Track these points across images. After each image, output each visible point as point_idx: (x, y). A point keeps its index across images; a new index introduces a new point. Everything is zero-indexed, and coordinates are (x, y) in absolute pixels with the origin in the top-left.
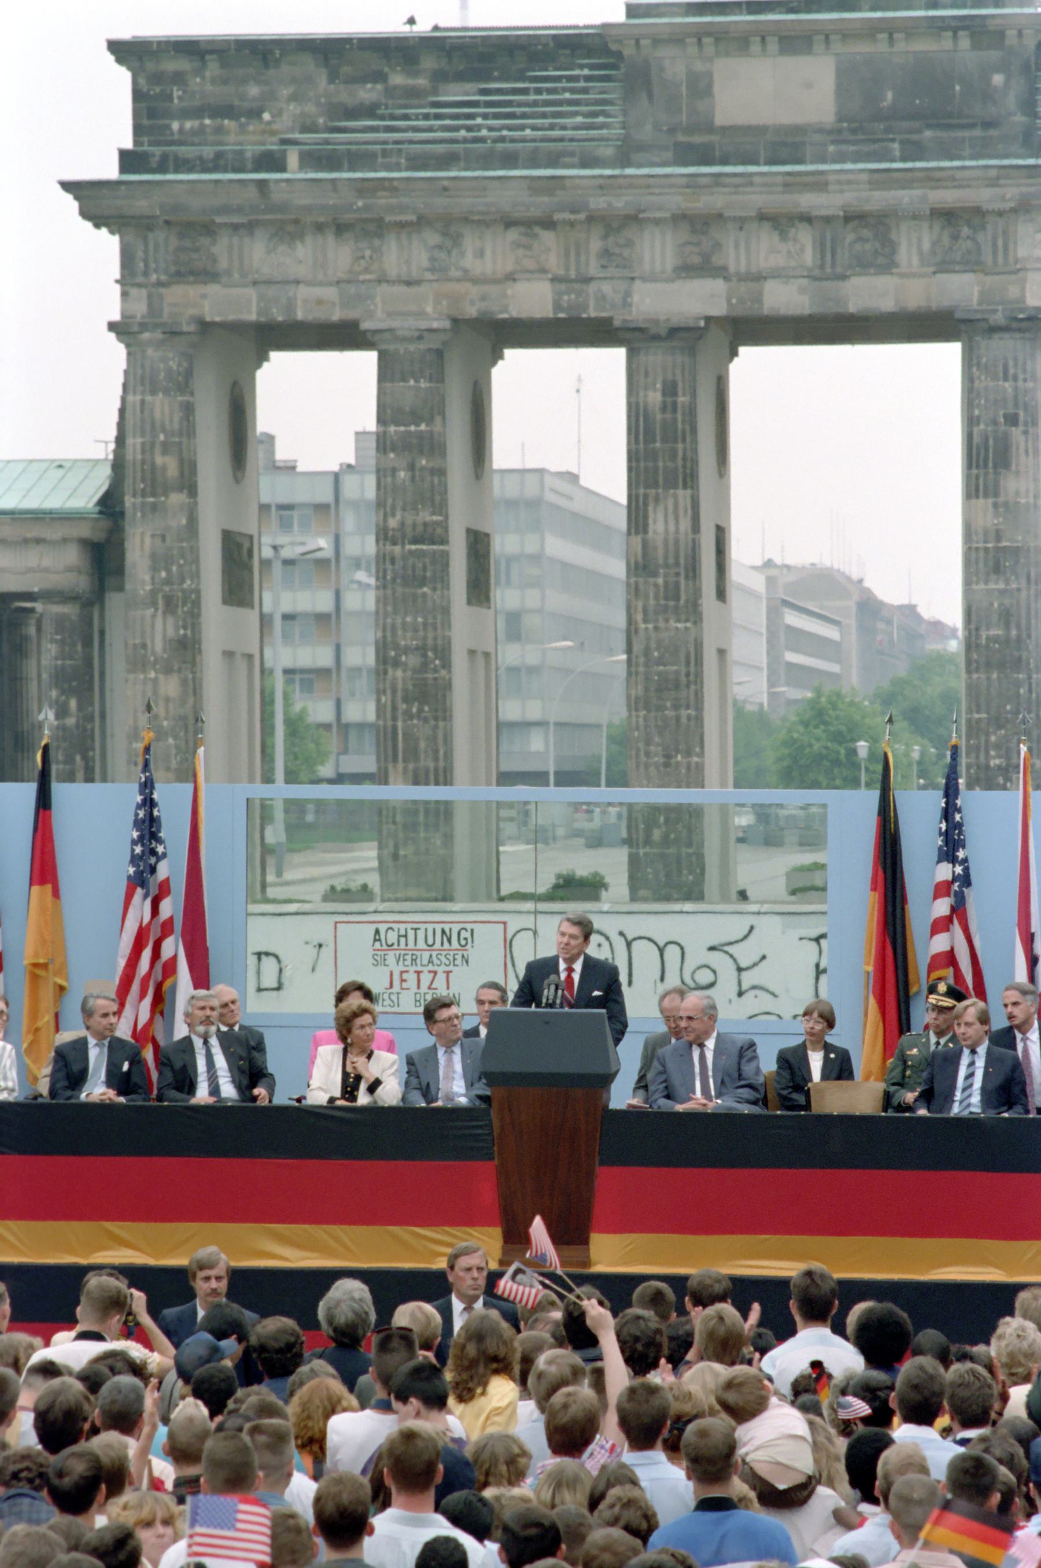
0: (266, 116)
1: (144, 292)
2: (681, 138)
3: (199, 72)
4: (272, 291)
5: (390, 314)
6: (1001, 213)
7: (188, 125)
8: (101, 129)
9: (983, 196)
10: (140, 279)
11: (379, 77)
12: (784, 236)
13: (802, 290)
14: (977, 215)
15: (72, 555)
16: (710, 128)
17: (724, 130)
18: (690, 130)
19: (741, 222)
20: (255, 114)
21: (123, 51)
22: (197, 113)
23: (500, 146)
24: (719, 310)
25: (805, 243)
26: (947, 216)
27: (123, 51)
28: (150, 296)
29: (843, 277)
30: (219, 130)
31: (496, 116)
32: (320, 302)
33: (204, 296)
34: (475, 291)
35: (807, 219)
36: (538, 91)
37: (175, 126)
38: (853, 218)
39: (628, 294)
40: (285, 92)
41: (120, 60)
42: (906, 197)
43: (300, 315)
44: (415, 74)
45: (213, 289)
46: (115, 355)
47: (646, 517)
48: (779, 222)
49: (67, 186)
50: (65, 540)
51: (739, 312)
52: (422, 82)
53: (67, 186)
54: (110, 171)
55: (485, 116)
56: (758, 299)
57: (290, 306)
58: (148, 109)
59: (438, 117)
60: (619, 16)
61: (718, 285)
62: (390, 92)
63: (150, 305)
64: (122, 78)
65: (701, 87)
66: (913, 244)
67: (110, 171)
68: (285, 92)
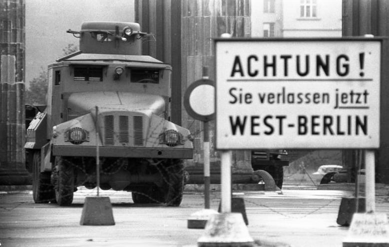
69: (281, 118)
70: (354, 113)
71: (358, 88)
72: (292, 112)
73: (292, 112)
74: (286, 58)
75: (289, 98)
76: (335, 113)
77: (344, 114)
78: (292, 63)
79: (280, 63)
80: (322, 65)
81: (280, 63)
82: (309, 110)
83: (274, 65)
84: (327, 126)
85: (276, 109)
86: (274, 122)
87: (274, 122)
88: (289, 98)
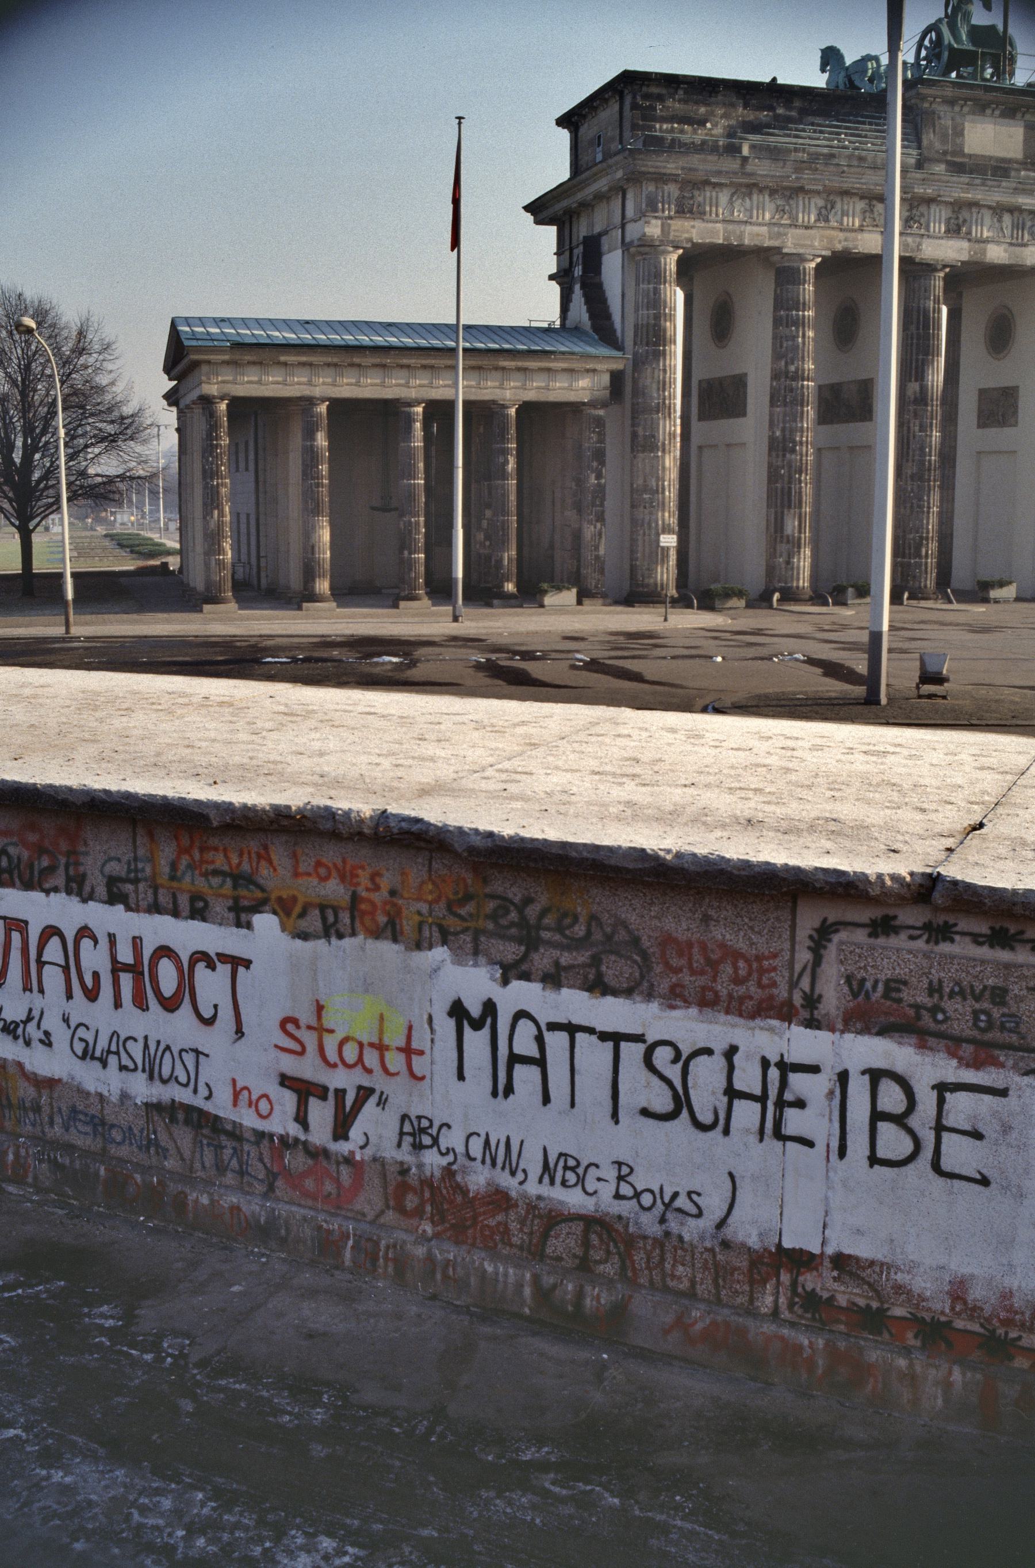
0: (708, 125)
1: (659, 222)
2: (949, 158)
3: (672, 96)
4: (730, 227)
5: (795, 245)
7: (665, 126)
10: (660, 214)
11: (771, 108)
13: (1006, 251)
16: (964, 155)
17: (970, 156)
18: (954, 153)
20: (702, 123)
22: (671, 119)
23: (857, 152)
24: (965, 257)
28: (663, 225)
29: (1025, 245)
30: (682, 132)
31: (852, 135)
32: (758, 235)
33: (693, 227)
34: (842, 235)
36: (870, 124)
37: (658, 126)
39: (920, 244)
40: (720, 112)
43: (746, 242)
44: (790, 109)
45: (698, 224)
47: (923, 372)
48: (999, 210)
51: (974, 259)
52: (794, 114)
55: (846, 134)
56: (984, 252)
57: (741, 236)
59: (821, 132)
61: (965, 244)
62: (777, 117)
63: (662, 230)
65: (959, 133)
68: (720, 112)
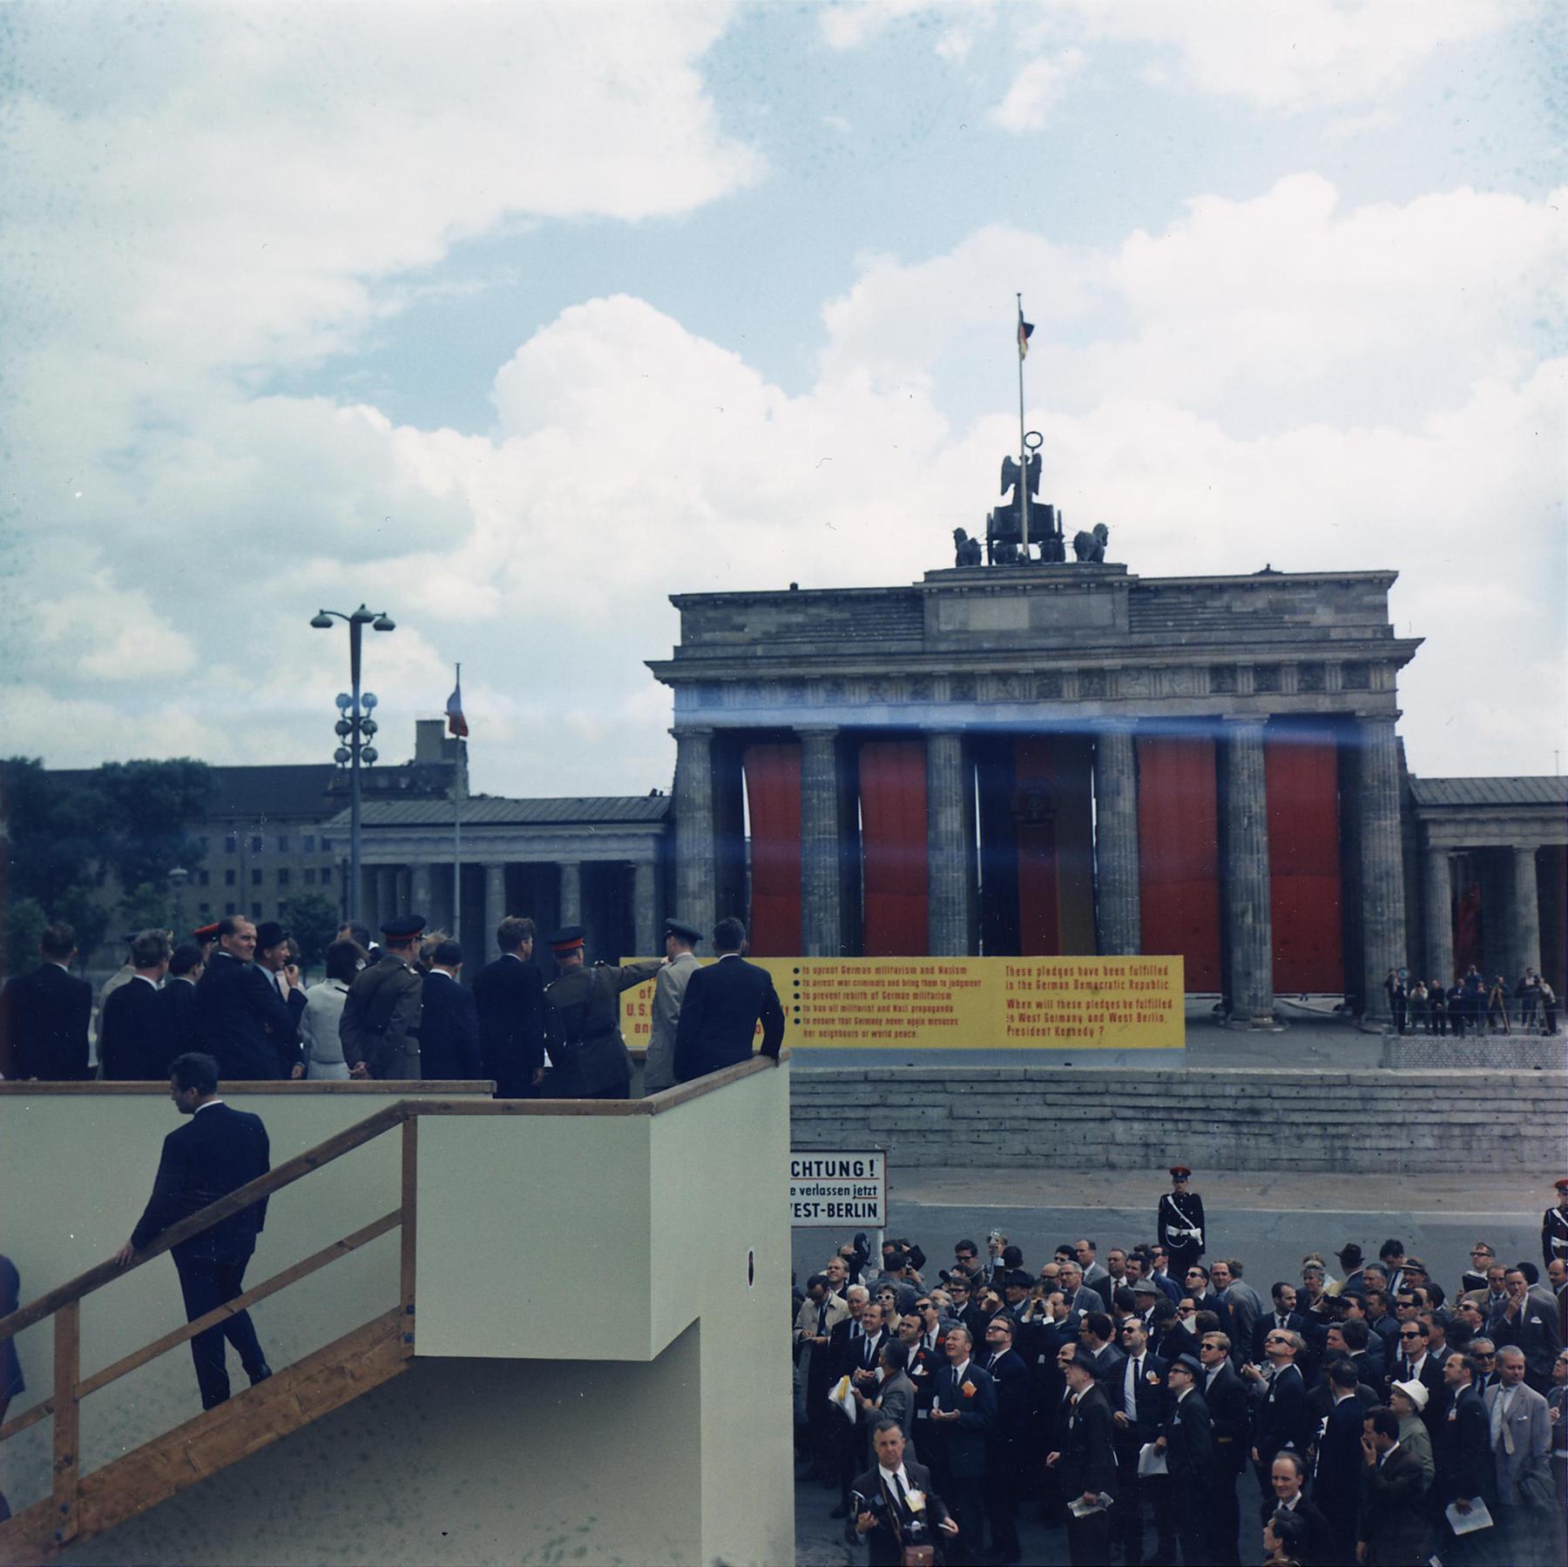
6: (1113, 671)
8: (666, 636)
9: (1107, 663)
12: (1005, 684)
14: (1101, 673)
15: (650, 843)
19: (984, 677)
20: (741, 628)
21: (676, 600)
25: (1016, 688)
26: (1085, 673)
27: (676, 600)
35: (1016, 674)
38: (1039, 674)
41: (675, 605)
42: (1064, 664)
46: (673, 744)
49: (648, 663)
50: (647, 835)
53: (648, 663)
54: (670, 656)
58: (687, 627)
60: (921, 579)
64: (676, 614)
66: (1070, 689)
67: (669, 656)
69: (816, 1205)
70: (867, 1202)
71: (870, 1184)
72: (823, 1201)
73: (823, 1201)
74: (818, 1163)
75: (822, 1192)
76: (853, 1202)
77: (860, 1203)
78: (823, 1167)
79: (814, 1167)
80: (844, 1168)
81: (814, 1167)
82: (835, 1200)
83: (810, 1168)
84: (848, 1211)
85: (813, 1199)
86: (811, 1208)
87: (811, 1208)
88: (822, 1192)
